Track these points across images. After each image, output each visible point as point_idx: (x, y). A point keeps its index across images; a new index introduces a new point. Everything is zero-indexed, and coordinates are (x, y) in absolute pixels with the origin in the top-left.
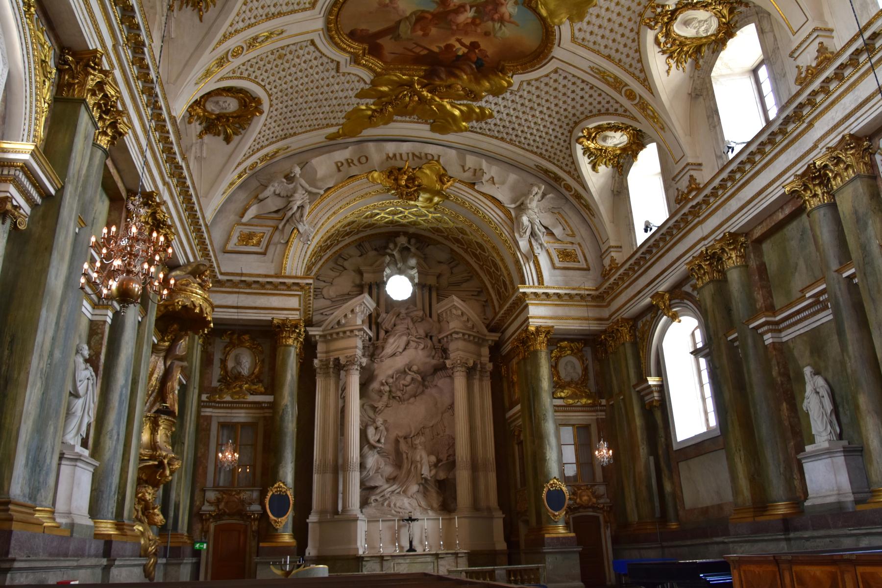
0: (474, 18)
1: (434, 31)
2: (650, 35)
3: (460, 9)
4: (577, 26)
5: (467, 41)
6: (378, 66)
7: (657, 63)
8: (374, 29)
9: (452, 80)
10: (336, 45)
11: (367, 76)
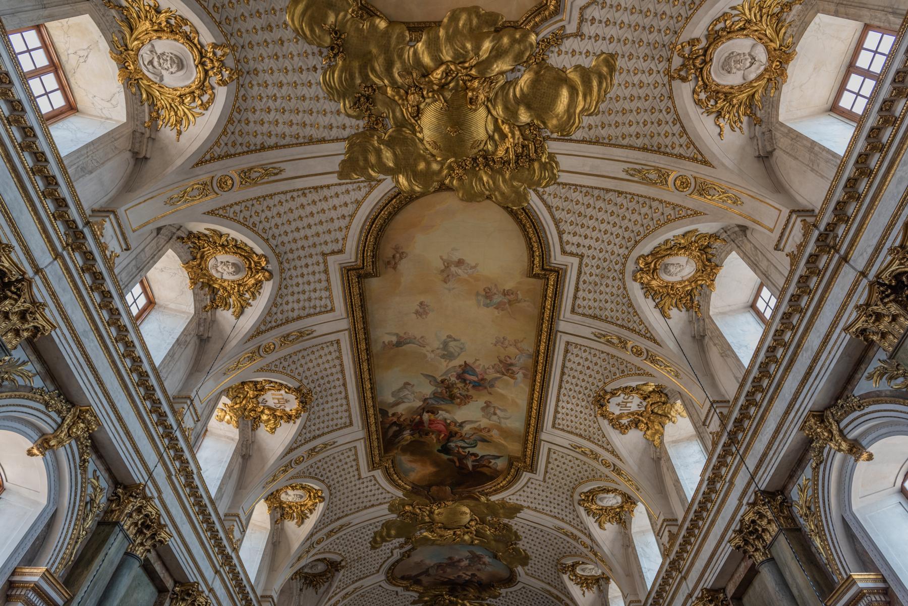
0: (469, 565)
1: (449, 570)
2: (565, 577)
3: (460, 561)
4: (526, 568)
5: (469, 573)
6: (421, 589)
7: (575, 590)
8: (414, 573)
9: (466, 593)
10: (395, 585)
11: (416, 595)
